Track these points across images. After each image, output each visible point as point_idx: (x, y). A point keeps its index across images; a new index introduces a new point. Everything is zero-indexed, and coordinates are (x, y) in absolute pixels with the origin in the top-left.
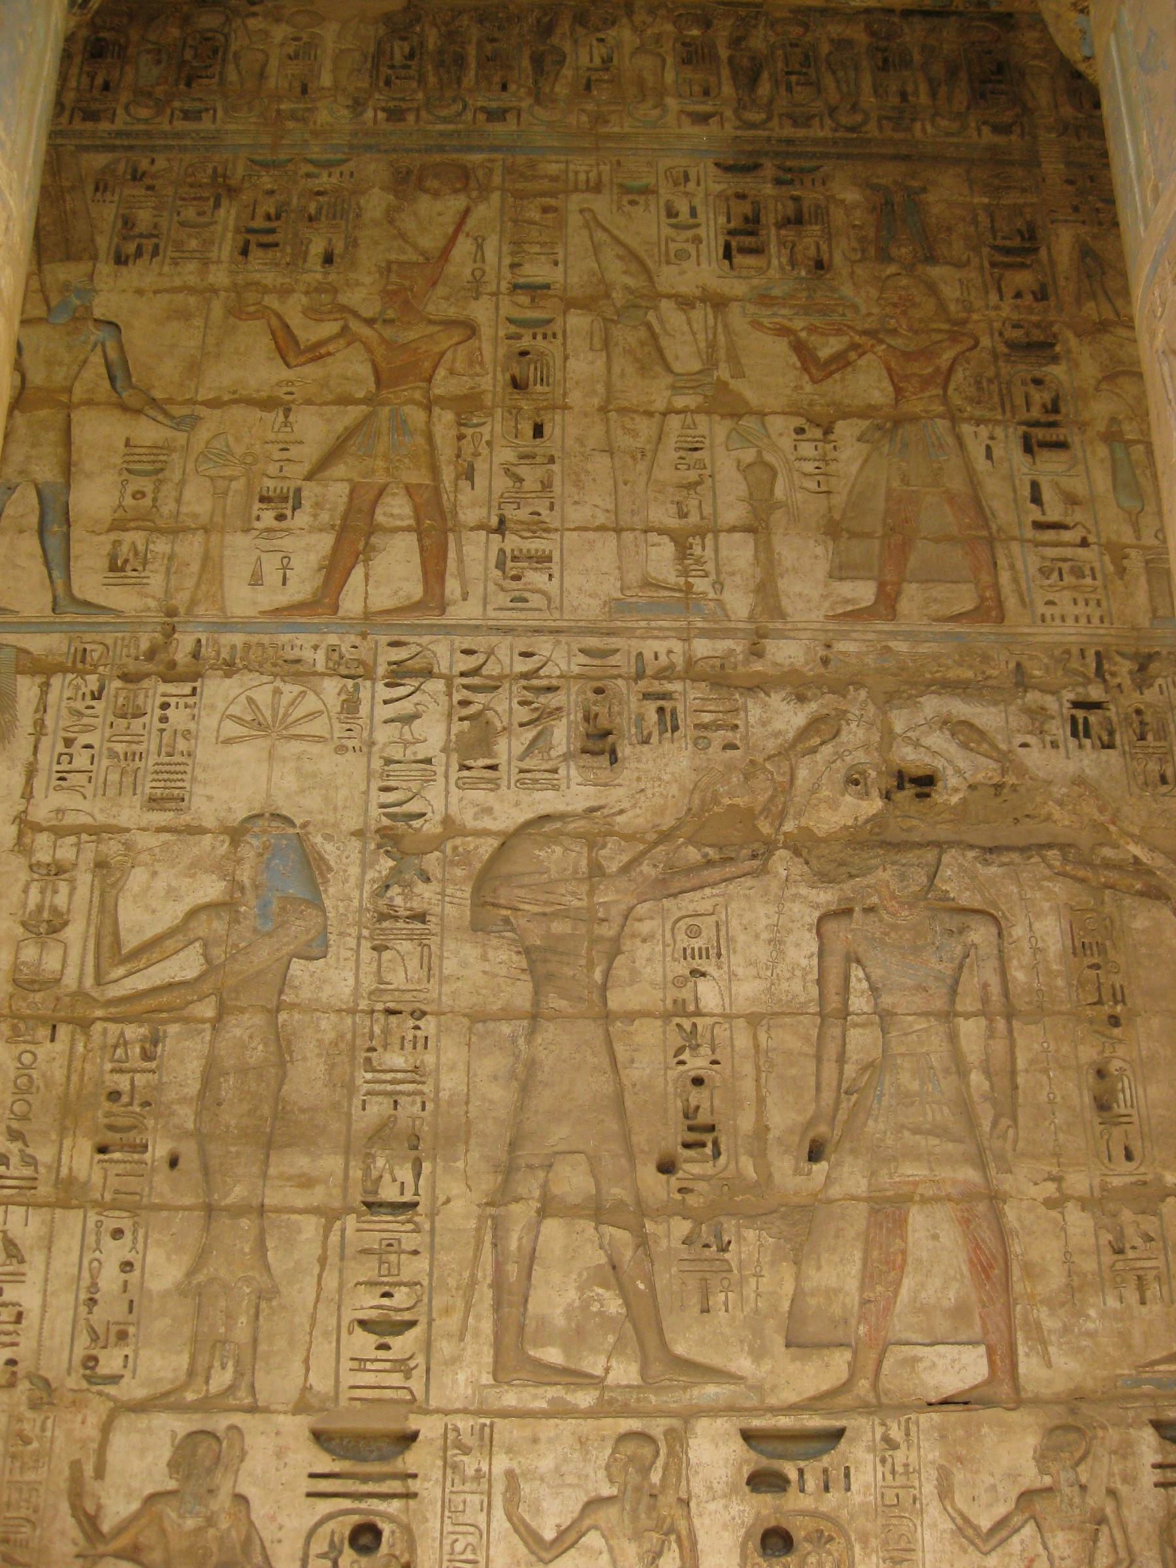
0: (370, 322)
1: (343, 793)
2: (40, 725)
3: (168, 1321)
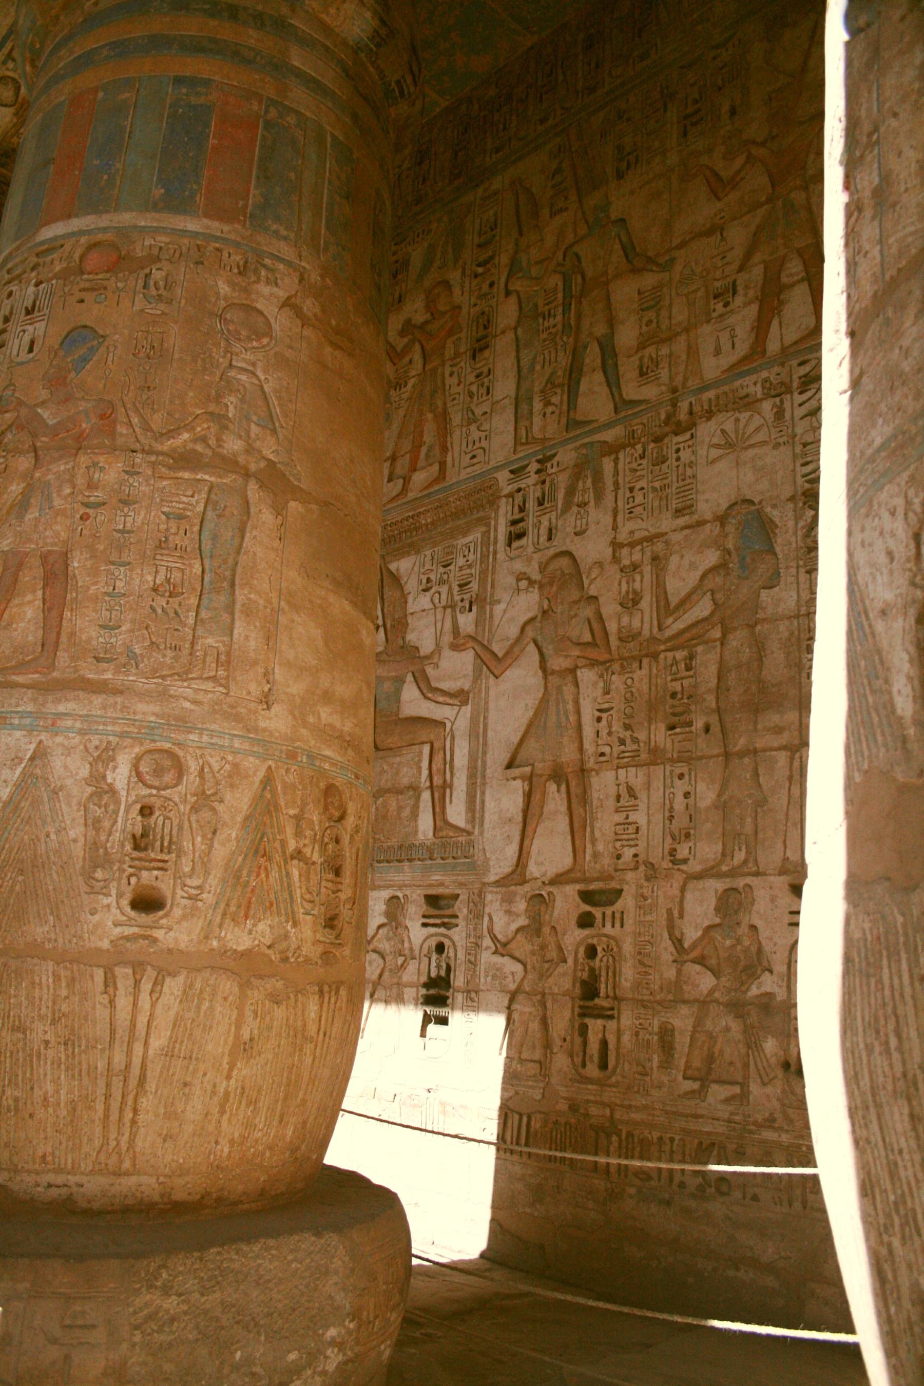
0: (763, 144)
1: (781, 473)
2: (616, 484)
3: (709, 825)
